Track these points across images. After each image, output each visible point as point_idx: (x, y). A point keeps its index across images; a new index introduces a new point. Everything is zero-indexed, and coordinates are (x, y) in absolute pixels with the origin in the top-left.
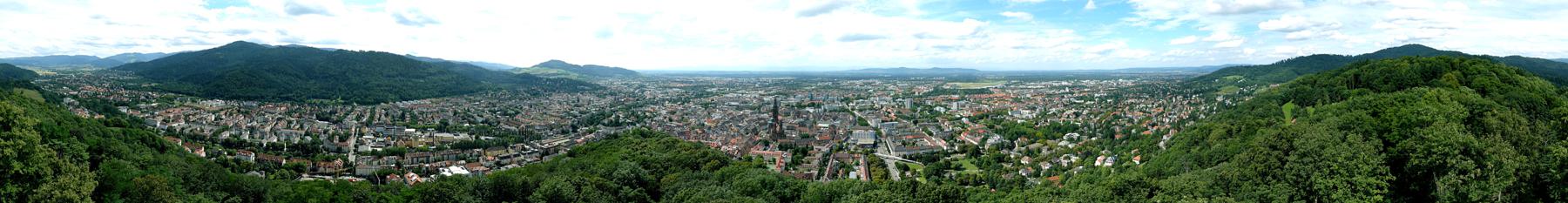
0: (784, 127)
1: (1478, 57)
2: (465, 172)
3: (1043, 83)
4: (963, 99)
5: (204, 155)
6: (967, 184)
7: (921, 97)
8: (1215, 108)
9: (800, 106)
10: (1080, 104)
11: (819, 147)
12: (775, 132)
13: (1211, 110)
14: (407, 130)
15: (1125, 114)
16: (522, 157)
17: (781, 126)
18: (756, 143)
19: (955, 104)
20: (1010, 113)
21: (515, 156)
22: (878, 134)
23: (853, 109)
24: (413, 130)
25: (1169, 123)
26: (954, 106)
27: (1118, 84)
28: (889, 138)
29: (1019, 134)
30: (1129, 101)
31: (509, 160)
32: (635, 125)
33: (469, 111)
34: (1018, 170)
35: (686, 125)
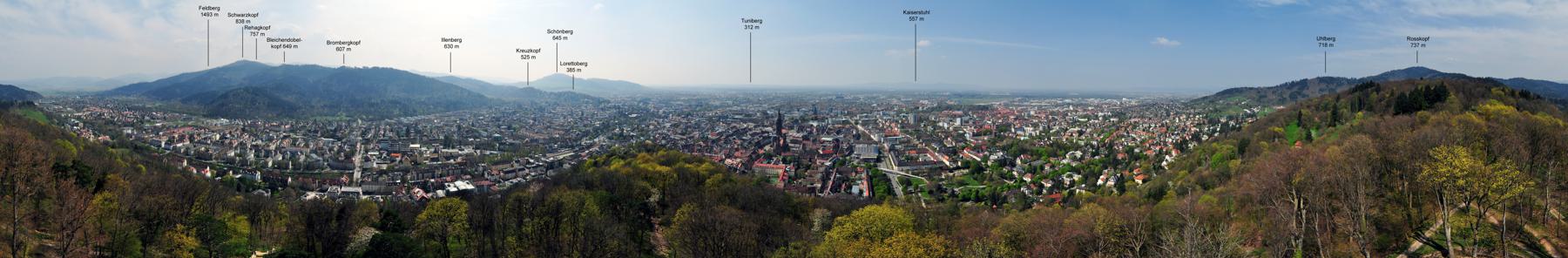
0: (788, 141)
1: (1470, 79)
2: (470, 187)
3: (1047, 101)
4: (966, 114)
5: (209, 174)
6: (968, 200)
7: (925, 112)
8: (1218, 129)
9: (803, 120)
10: (1083, 122)
11: (822, 161)
12: (778, 145)
13: (1214, 131)
14: (412, 146)
15: (1128, 133)
16: (527, 171)
17: (785, 139)
18: (758, 157)
19: (958, 120)
20: (1013, 130)
21: (520, 170)
22: (879, 151)
23: (857, 123)
24: (418, 146)
25: (1172, 143)
26: (958, 122)
27: (1121, 103)
28: (892, 153)
29: (1024, 151)
30: (1133, 120)
31: (514, 174)
32: (639, 138)
33: (473, 125)
34: (1020, 187)
35: (690, 138)
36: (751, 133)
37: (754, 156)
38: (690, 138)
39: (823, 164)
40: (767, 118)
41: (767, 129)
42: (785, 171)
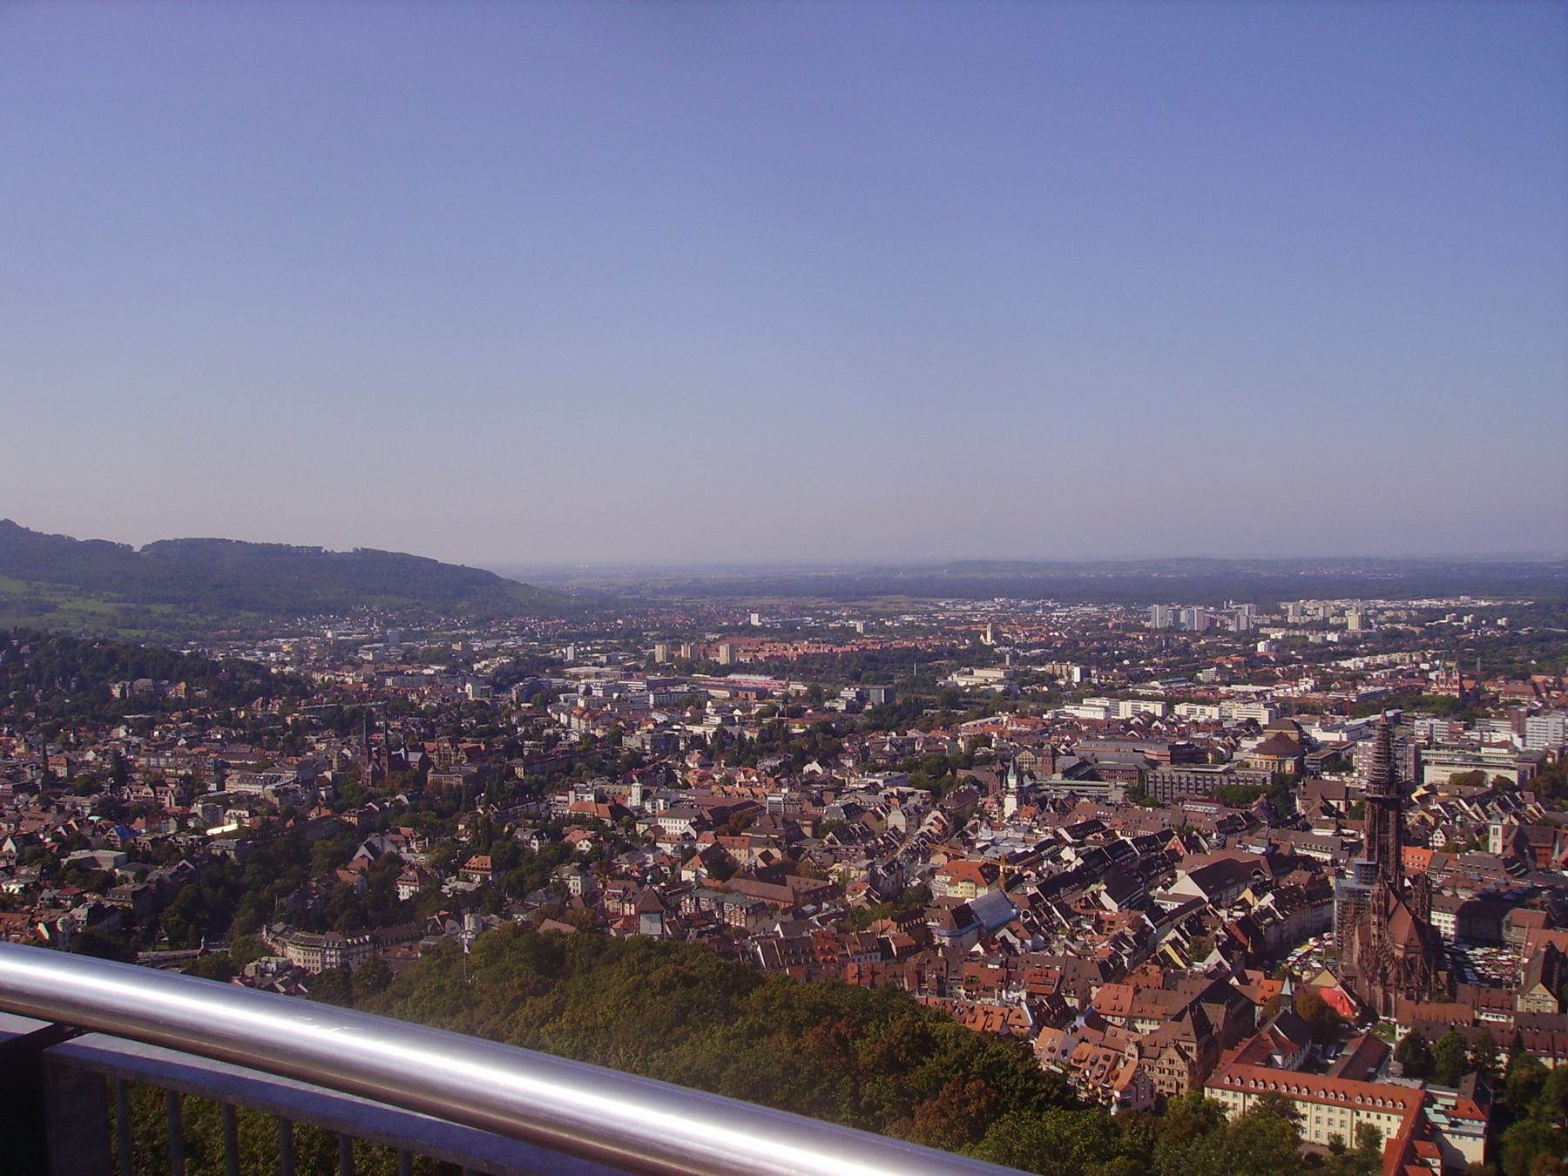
37: (1217, 1014)
38: (816, 897)
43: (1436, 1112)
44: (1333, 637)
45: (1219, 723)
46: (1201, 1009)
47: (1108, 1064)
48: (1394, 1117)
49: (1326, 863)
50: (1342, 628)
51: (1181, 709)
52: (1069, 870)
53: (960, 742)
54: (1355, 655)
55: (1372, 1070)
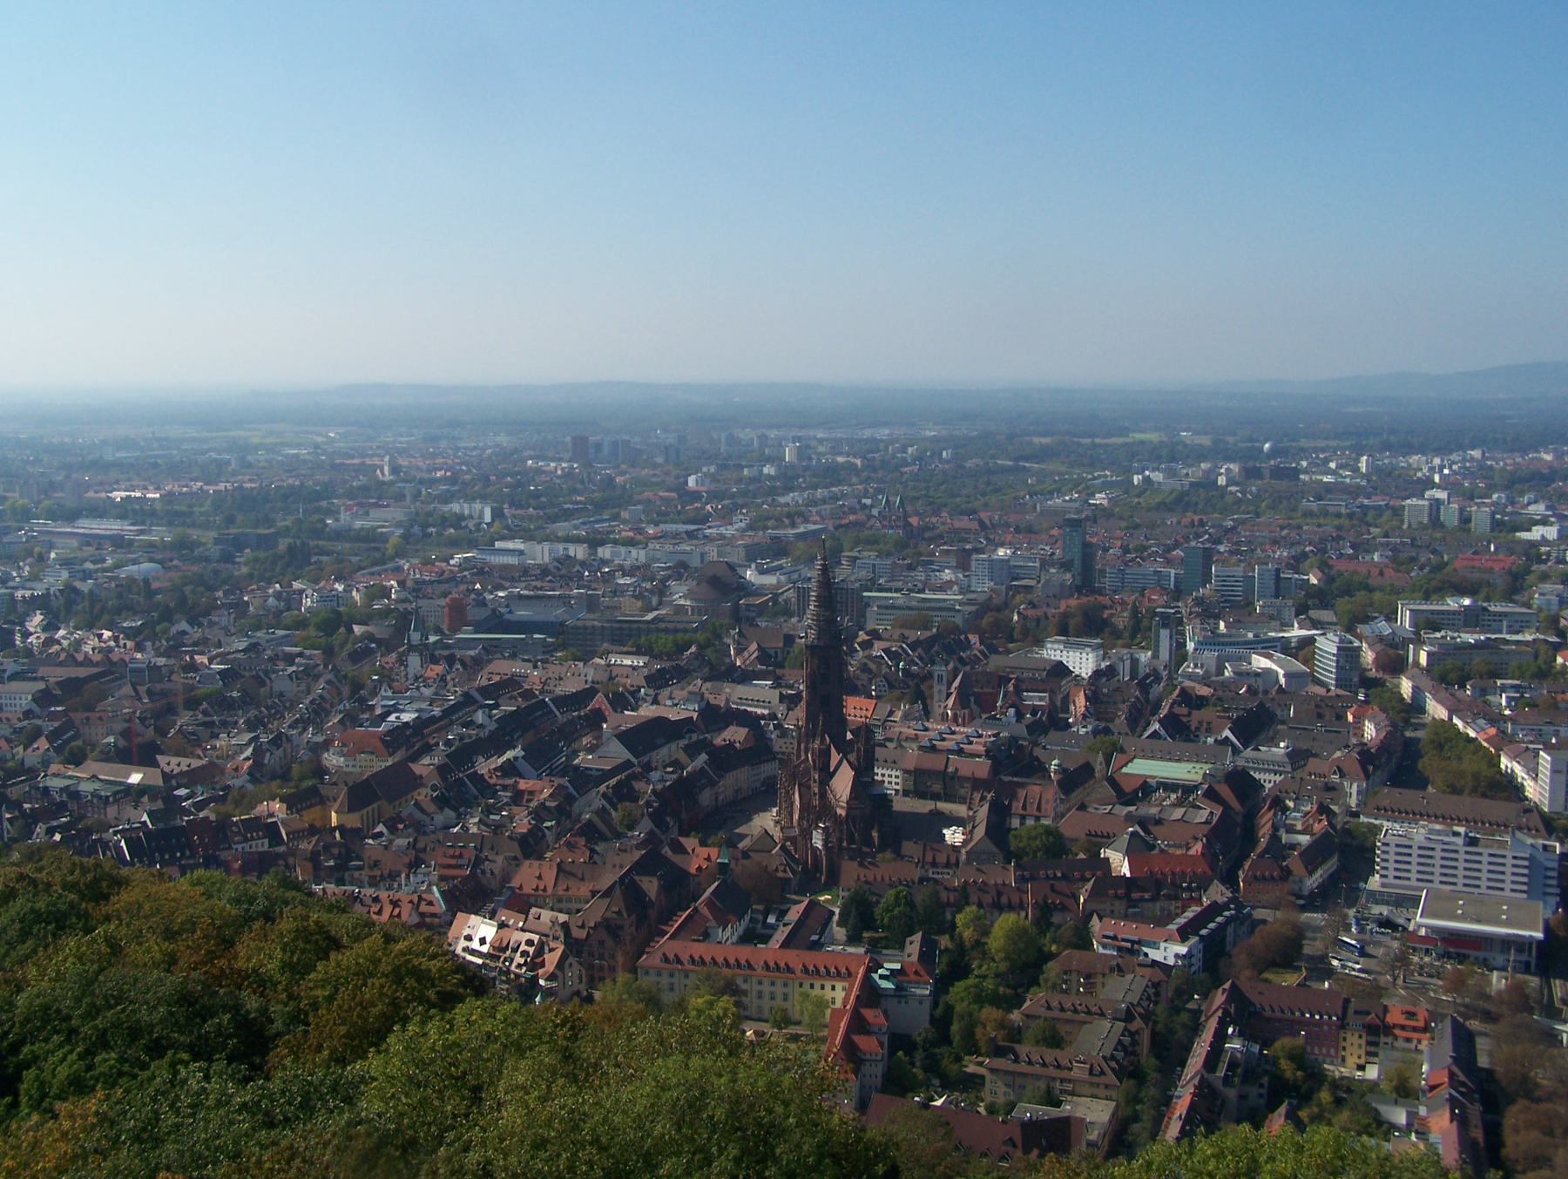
11: (1129, 930)
36: (631, 717)
39: (1132, 950)
40: (739, 617)
41: (734, 695)
42: (870, 995)
43: (882, 977)
44: (768, 470)
45: (647, 566)
46: (633, 882)
47: (531, 950)
48: (839, 985)
49: (763, 717)
50: (777, 459)
51: (605, 552)
52: (482, 735)
53: (354, 593)
54: (791, 489)
55: (815, 938)
